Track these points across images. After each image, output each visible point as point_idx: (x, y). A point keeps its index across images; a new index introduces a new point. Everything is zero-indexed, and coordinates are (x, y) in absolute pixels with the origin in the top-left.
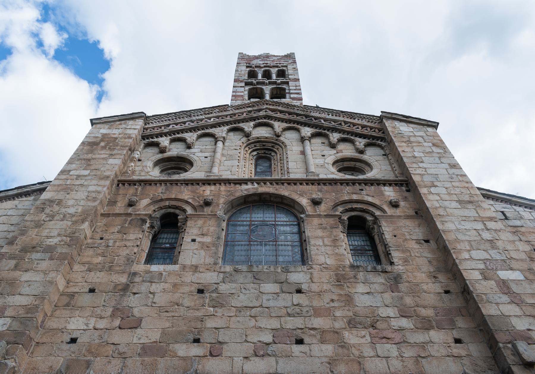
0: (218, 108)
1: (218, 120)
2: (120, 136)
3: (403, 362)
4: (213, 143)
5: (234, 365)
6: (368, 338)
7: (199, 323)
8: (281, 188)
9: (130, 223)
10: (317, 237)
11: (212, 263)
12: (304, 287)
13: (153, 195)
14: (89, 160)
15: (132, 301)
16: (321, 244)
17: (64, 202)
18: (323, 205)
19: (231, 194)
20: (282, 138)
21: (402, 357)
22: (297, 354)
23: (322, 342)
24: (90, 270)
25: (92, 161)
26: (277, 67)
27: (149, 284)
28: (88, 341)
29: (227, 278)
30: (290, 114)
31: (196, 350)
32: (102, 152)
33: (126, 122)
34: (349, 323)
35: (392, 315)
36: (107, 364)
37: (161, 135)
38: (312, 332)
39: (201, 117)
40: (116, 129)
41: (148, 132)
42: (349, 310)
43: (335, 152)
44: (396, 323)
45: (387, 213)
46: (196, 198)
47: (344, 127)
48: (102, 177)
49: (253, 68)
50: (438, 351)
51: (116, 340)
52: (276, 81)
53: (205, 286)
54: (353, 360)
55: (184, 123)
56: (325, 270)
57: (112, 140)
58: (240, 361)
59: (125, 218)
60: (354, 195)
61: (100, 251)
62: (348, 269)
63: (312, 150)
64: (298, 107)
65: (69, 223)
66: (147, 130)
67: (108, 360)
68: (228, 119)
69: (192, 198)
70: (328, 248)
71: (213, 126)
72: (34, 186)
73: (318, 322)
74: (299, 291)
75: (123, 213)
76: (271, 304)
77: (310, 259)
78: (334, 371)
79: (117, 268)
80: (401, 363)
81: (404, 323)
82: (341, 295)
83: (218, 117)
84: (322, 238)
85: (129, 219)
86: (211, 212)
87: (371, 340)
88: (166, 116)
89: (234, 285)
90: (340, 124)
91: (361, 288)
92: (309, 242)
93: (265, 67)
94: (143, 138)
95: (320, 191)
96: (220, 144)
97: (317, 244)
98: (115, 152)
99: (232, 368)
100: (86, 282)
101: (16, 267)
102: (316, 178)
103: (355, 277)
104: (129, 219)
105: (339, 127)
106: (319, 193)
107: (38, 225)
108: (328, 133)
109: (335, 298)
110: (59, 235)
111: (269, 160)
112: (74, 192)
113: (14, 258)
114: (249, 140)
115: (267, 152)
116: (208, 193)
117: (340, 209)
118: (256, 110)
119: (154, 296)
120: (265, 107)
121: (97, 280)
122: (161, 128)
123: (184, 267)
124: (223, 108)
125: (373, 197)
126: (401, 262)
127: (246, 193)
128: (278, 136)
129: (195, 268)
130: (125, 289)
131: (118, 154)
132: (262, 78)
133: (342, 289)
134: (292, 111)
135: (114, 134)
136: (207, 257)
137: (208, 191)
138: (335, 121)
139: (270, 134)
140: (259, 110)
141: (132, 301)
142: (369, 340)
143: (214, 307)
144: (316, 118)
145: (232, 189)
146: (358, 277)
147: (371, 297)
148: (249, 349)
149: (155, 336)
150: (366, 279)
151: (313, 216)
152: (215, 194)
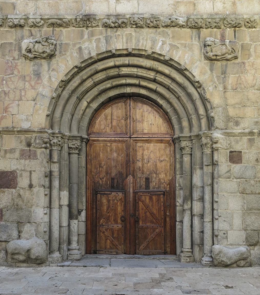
3: (224, 3)
5: (110, 6)
36: (26, 6)
58: (113, 3)
67: (26, 3)
78: (176, 11)
80: (223, 5)
99: (109, 8)
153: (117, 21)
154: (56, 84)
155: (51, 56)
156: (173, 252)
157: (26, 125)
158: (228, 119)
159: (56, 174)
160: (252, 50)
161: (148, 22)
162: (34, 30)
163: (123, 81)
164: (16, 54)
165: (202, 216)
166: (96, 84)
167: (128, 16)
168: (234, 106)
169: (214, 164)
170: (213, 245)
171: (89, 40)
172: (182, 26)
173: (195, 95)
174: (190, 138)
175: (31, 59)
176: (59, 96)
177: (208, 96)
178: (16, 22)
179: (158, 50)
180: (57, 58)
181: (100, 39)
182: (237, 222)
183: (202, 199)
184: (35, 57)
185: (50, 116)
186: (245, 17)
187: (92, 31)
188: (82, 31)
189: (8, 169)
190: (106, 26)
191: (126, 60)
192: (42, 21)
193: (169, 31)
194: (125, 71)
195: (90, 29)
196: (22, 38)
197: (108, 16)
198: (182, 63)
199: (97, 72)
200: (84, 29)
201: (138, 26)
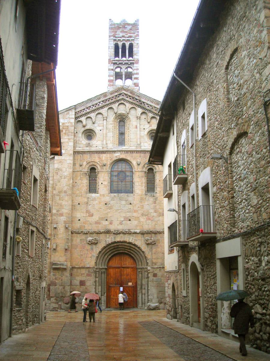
2: (69, 124)
4: (103, 120)
8: (127, 155)
12: (132, 202)
15: (90, 207)
23: (135, 220)
24: (76, 196)
29: (113, 199)
31: (107, 223)
32: (65, 137)
33: (68, 112)
34: (142, 214)
35: (152, 212)
37: (81, 116)
38: (133, 217)
39: (96, 102)
41: (77, 115)
43: (148, 126)
44: (152, 214)
49: (117, 41)
51: (89, 220)
62: (144, 195)
65: (67, 180)
68: (108, 102)
70: (140, 187)
71: (102, 107)
73: (135, 214)
74: (131, 204)
76: (124, 208)
81: (155, 214)
83: (103, 101)
84: (139, 182)
85: (82, 173)
93: (123, 40)
94: (76, 118)
96: (105, 121)
98: (70, 137)
101: (60, 199)
103: (145, 199)
104: (82, 173)
107: (59, 182)
109: (139, 206)
110: (66, 186)
111: (124, 122)
116: (104, 158)
118: (119, 95)
122: (81, 111)
124: (105, 95)
128: (128, 114)
129: (104, 195)
130: (87, 203)
134: (134, 96)
135: (66, 123)
137: (104, 156)
138: (151, 106)
139: (125, 111)
141: (90, 207)
144: (144, 103)
148: (118, 222)
149: (97, 219)
151: (137, 171)
154: (98, 252)
155: (96, 243)
156: (137, 307)
157: (88, 266)
158: (153, 263)
159: (98, 281)
160: (160, 241)
162: (91, 235)
163: (119, 249)
164: (85, 242)
165: (145, 294)
166: (110, 250)
168: (155, 259)
169: (148, 277)
170: (148, 303)
171: (109, 238)
172: (138, 234)
173: (143, 255)
174: (141, 268)
175: (90, 244)
176: (99, 256)
177: (146, 255)
178: (86, 232)
179: (130, 241)
180: (98, 244)
182: (155, 296)
183: (145, 289)
184: (91, 244)
185: (96, 263)
186: (158, 230)
189: (83, 280)
190: (114, 233)
191: (121, 244)
193: (134, 235)
194: (120, 246)
196: (87, 237)
197: (115, 231)
198: (138, 245)
199: (111, 247)
201: (123, 233)
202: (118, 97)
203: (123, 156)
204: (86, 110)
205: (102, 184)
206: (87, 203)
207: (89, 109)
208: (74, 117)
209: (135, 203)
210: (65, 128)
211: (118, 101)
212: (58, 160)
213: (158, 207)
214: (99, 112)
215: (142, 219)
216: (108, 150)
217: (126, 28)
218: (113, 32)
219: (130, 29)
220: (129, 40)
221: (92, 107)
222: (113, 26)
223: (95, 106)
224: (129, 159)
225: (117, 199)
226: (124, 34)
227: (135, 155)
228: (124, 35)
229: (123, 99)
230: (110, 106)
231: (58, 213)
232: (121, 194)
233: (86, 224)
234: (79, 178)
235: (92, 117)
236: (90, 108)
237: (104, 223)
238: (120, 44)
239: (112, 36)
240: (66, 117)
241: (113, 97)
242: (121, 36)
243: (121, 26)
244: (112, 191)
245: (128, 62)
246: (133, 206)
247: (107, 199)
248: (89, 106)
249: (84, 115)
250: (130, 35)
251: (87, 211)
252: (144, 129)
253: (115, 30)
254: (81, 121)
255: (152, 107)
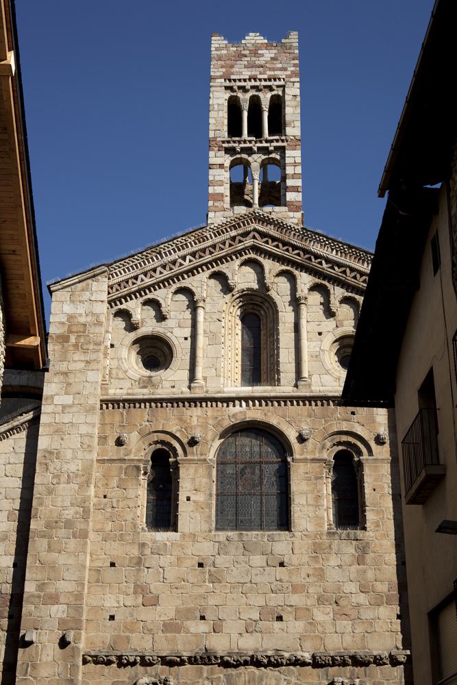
0: (193, 234)
1: (195, 261)
6: (331, 614)
7: (203, 600)
9: (125, 473)
10: (301, 493)
11: (207, 530)
12: (286, 560)
13: (140, 425)
14: (66, 374)
16: (305, 503)
17: (62, 453)
18: (311, 440)
19: (219, 424)
20: (273, 293)
21: (353, 632)
22: (277, 630)
25: (71, 376)
26: (270, 88)
27: (157, 556)
28: (123, 618)
29: (222, 549)
30: (285, 244)
31: (203, 627)
32: (76, 357)
33: (88, 285)
34: (318, 599)
35: (354, 591)
38: (289, 609)
39: (174, 256)
40: (80, 302)
41: (115, 295)
42: (320, 586)
44: (354, 600)
45: (373, 455)
46: (183, 430)
47: (349, 278)
48: (88, 408)
50: (381, 627)
52: (268, 147)
53: (203, 559)
54: (317, 636)
55: (154, 270)
56: (304, 538)
57: (82, 330)
59: (120, 465)
60: (344, 422)
61: (108, 515)
62: (325, 537)
63: (308, 322)
64: (295, 230)
65: (76, 487)
66: (112, 288)
68: (208, 258)
69: (181, 431)
70: (311, 508)
71: (191, 272)
72: (22, 417)
73: (295, 599)
74: (282, 564)
75: (116, 458)
77: (292, 524)
79: (128, 538)
81: (362, 599)
82: (315, 569)
83: (193, 254)
84: (306, 493)
86: (201, 455)
87: (334, 616)
88: (131, 259)
89: (228, 557)
90: (344, 272)
91: (334, 561)
92: (294, 500)
93: (253, 87)
94: (111, 303)
95: (310, 416)
96: (200, 312)
97: (301, 503)
100: (105, 554)
101: (50, 549)
102: (308, 394)
104: (124, 466)
105: (342, 277)
106: (308, 420)
108: (327, 284)
109: (311, 572)
110: (72, 505)
112: (67, 436)
113: (44, 536)
114: (233, 295)
115: (255, 308)
116: (195, 421)
117: (329, 444)
119: (164, 570)
120: (252, 228)
121: (114, 553)
122: (127, 282)
123: (184, 535)
125: (363, 425)
126: (372, 527)
127: (234, 421)
129: (193, 536)
130: (139, 562)
131: (94, 360)
132: (248, 136)
133: (317, 562)
134: (286, 239)
135: (81, 315)
136: (202, 521)
137: (195, 413)
138: (340, 265)
140: (246, 234)
141: (147, 577)
142: (332, 617)
143: (213, 582)
144: (317, 256)
145: (219, 414)
146: (333, 546)
147: (340, 570)
149: (172, 614)
150: (339, 549)
152: (203, 423)
153: (239, 659)
161: (272, 660)
167: (251, 653)
181: (220, 677)
187: (212, 669)
188: (202, 669)
192: (159, 659)
195: (210, 666)
200: (203, 666)
202: (240, 241)
203: (255, 413)
204: (142, 280)
205: (188, 499)
206: (139, 562)
207: (151, 277)
208: (105, 297)
209: (295, 560)
210: (75, 329)
211: (239, 253)
212: (50, 425)
213: (370, 575)
214: (183, 285)
215: (323, 615)
216: (208, 395)
217: (262, 55)
218: (222, 67)
219: (271, 58)
220: (270, 88)
221: (162, 270)
222: (224, 52)
223: (171, 269)
224: (274, 421)
225: (237, 548)
226: (255, 72)
227: (293, 410)
228: (253, 73)
229: (255, 249)
230: (216, 269)
231: (42, 594)
232: (249, 533)
233: (132, 631)
234: (114, 482)
235: (159, 299)
236: (153, 274)
237: (192, 630)
238: (245, 98)
239: (220, 77)
240: (81, 299)
241: (224, 243)
242: (248, 77)
243: (247, 52)
244: (223, 523)
245: (268, 145)
246: (290, 572)
247: (206, 549)
248: (152, 267)
249: (134, 293)
250: (272, 73)
251: (140, 589)
252: (320, 334)
253: (228, 62)
254: (125, 315)
255: (340, 270)
